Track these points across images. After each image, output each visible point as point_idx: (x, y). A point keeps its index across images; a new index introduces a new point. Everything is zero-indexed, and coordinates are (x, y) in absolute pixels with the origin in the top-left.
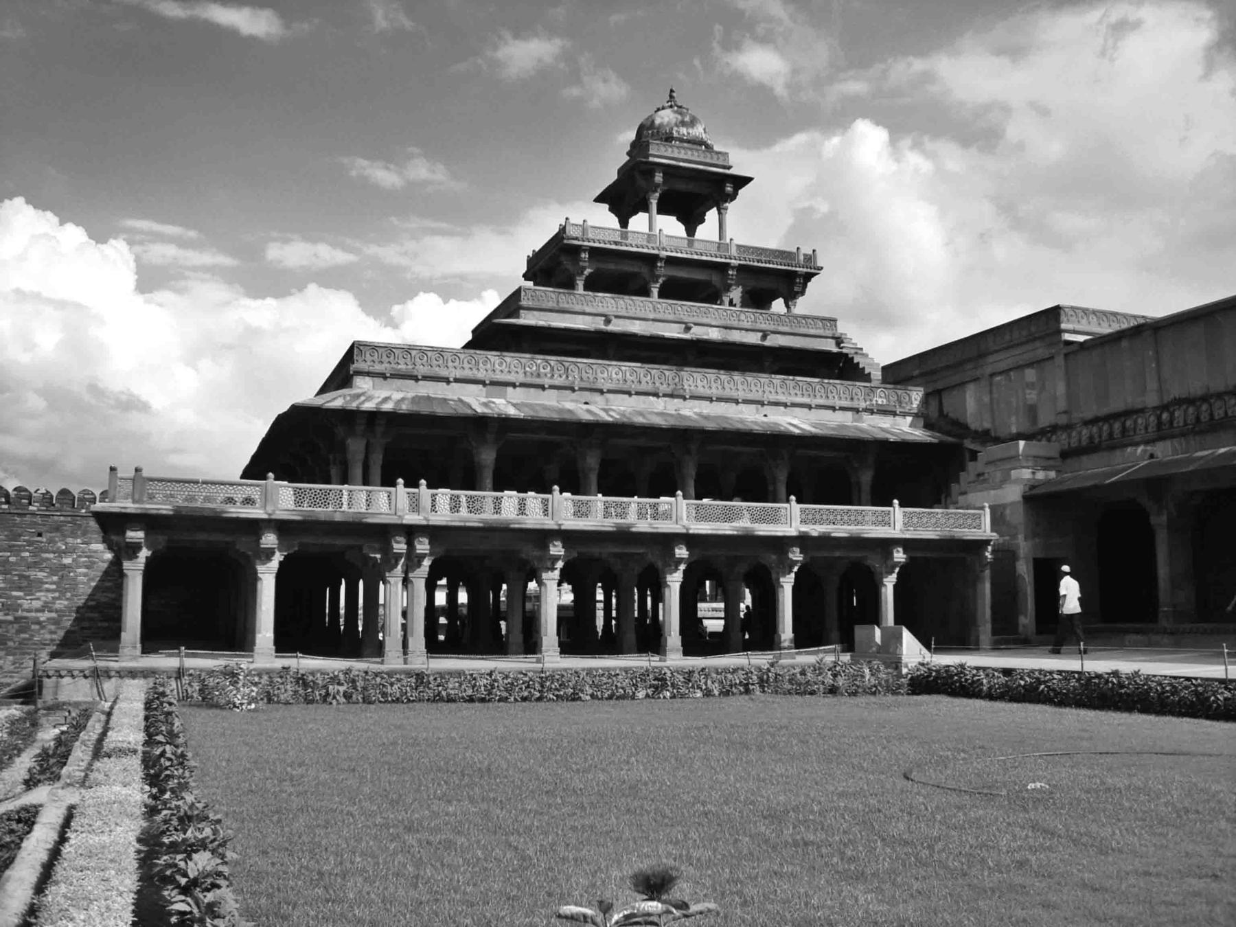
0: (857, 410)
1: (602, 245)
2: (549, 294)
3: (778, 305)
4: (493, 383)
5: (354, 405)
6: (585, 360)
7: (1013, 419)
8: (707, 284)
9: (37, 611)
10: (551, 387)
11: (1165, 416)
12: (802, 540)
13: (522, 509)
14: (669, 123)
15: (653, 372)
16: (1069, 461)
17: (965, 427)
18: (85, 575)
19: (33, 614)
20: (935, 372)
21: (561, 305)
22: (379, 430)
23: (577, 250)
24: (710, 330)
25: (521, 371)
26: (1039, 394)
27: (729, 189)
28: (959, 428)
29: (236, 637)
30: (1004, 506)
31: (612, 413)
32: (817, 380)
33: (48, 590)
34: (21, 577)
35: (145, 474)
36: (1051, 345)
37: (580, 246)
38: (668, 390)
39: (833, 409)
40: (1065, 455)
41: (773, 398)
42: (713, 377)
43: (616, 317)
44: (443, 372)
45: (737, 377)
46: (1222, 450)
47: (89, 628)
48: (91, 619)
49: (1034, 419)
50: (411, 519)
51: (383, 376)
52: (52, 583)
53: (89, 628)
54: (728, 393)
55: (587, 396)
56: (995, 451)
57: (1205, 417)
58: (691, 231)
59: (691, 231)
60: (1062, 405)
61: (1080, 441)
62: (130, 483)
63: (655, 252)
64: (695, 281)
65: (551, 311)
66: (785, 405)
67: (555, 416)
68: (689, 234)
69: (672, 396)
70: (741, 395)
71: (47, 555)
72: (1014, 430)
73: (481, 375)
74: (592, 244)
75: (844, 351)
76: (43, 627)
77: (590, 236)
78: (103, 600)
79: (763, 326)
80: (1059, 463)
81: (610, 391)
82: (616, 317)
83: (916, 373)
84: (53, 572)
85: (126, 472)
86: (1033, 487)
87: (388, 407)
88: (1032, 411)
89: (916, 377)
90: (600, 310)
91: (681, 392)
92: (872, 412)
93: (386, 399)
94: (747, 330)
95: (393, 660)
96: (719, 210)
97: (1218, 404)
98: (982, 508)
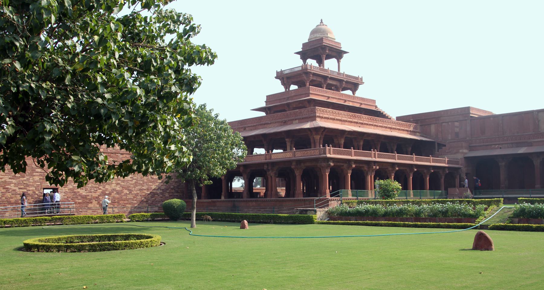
22: (324, 133)
88: (457, 134)
96: (339, 62)
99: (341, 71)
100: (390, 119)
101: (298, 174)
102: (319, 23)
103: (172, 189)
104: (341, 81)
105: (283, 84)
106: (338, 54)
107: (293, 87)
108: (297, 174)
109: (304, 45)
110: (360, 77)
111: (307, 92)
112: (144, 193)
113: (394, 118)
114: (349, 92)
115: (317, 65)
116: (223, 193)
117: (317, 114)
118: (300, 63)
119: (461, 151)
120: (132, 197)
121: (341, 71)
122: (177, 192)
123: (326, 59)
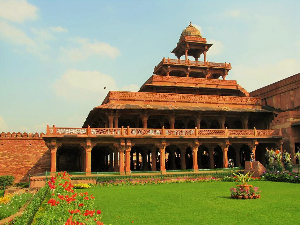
0: (243, 104)
1: (173, 64)
2: (160, 77)
3: (221, 78)
4: (146, 101)
5: (110, 108)
6: (170, 94)
8: (202, 73)
9: (30, 164)
10: (161, 101)
12: (230, 139)
13: (155, 133)
14: (190, 31)
15: (188, 96)
17: (274, 108)
19: (29, 165)
20: (265, 94)
21: (163, 80)
22: (117, 114)
23: (166, 66)
24: (203, 85)
25: (153, 97)
27: (206, 48)
28: (272, 108)
29: (80, 169)
30: (285, 129)
31: (177, 107)
32: (232, 97)
33: (33, 159)
34: (26, 156)
35: (56, 127)
38: (192, 101)
39: (236, 104)
41: (220, 102)
42: (204, 97)
43: (178, 82)
44: (133, 98)
45: (210, 96)
47: (44, 168)
48: (44, 166)
49: (293, 105)
50: (126, 136)
51: (117, 100)
54: (208, 101)
55: (171, 103)
56: (282, 114)
58: (196, 59)
59: (196, 59)
62: (52, 129)
63: (187, 65)
64: (199, 72)
66: (223, 104)
67: (163, 108)
68: (196, 60)
69: (193, 102)
70: (212, 102)
71: (32, 150)
72: (287, 108)
73: (143, 99)
74: (171, 64)
75: (239, 89)
77: (170, 62)
79: (217, 84)
81: (177, 102)
82: (178, 82)
84: (34, 154)
85: (51, 126)
86: (293, 123)
87: (119, 108)
88: (292, 103)
89: (259, 95)
90: (173, 81)
91: (196, 101)
92: (247, 105)
93: (118, 106)
94: (212, 85)
95: (122, 174)
96: (204, 53)
103: (44, 163)
104: (205, 69)
111: (151, 81)
112: (19, 167)
119: (288, 120)
120: (9, 170)
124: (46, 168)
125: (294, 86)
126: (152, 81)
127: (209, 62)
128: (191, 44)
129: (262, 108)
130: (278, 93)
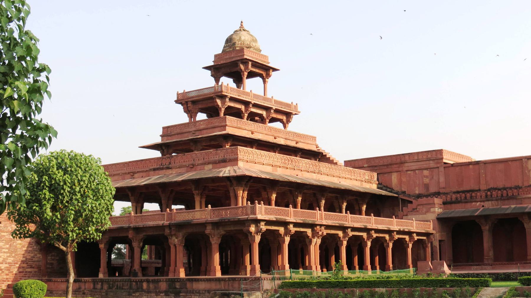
7: (417, 188)
8: (261, 116)
11: (489, 193)
16: (446, 205)
18: (20, 244)
26: (431, 180)
33: (4, 252)
36: (438, 163)
37: (227, 96)
40: (444, 203)
46: (513, 206)
47: (23, 272)
48: (23, 267)
52: (7, 248)
53: (23, 272)
57: (505, 195)
60: (442, 185)
61: (451, 199)
65: (236, 128)
71: (3, 234)
72: (417, 192)
76: (3, 272)
78: (28, 257)
80: (443, 206)
83: (365, 166)
86: (438, 215)
88: (427, 186)
90: (250, 129)
96: (265, 82)
97: (510, 191)
98: (430, 222)
99: (269, 96)
100: (336, 163)
101: (215, 242)
102: (237, 28)
105: (187, 111)
106: (264, 71)
107: (201, 116)
108: (213, 242)
109: (216, 56)
110: (294, 104)
111: (224, 124)
113: (341, 162)
114: (278, 125)
115: (234, 86)
116: (101, 269)
117: (240, 157)
118: (211, 82)
119: (432, 210)
121: (269, 96)
122: (31, 267)
123: (247, 78)
124: (26, 272)
125: (432, 164)
126: (226, 125)
127: (275, 98)
128: (255, 64)
129: (378, 188)
130: (402, 170)
